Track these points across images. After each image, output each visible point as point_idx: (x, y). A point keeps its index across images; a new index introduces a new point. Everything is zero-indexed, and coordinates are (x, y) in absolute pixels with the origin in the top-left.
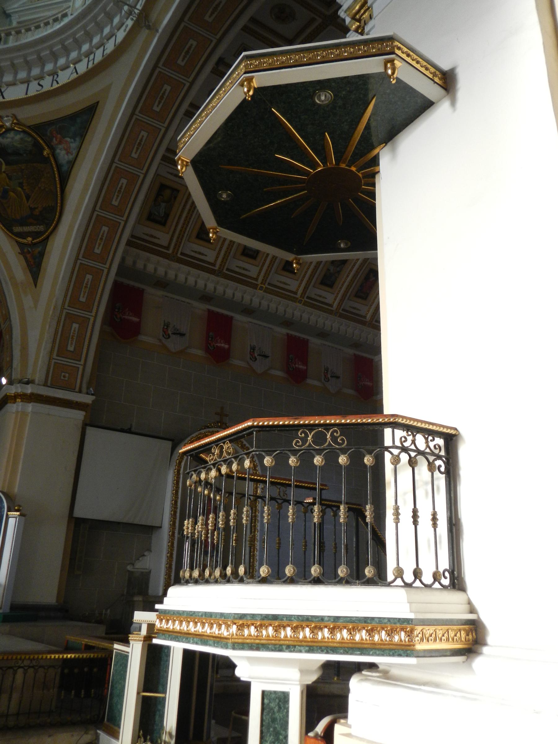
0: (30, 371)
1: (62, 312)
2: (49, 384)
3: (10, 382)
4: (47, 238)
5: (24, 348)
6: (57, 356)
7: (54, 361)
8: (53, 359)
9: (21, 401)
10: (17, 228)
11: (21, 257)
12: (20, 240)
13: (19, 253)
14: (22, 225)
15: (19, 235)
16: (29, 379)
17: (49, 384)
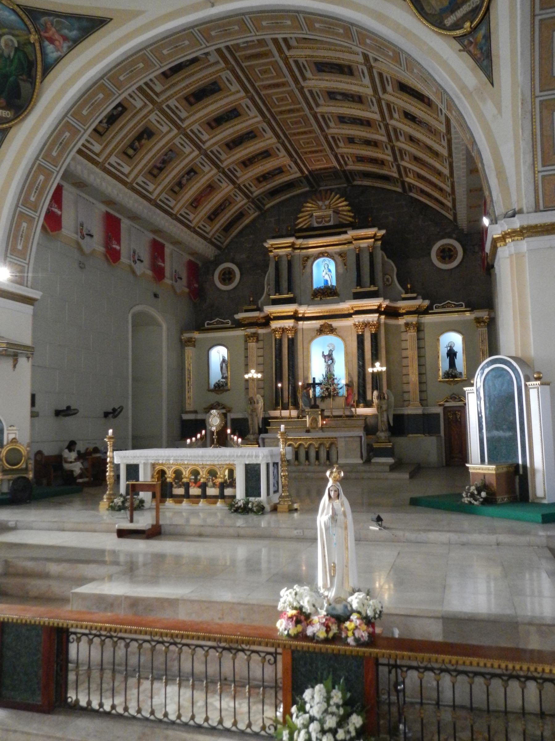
0: (514, 198)
1: (533, 104)
2: (542, 208)
3: (494, 221)
4: (488, 9)
5: (501, 173)
6: (543, 166)
7: (541, 174)
8: (539, 172)
9: (512, 241)
10: (449, 19)
11: (465, 53)
12: (459, 32)
13: (460, 51)
14: (452, 11)
15: (457, 26)
16: (514, 209)
17: (542, 208)
